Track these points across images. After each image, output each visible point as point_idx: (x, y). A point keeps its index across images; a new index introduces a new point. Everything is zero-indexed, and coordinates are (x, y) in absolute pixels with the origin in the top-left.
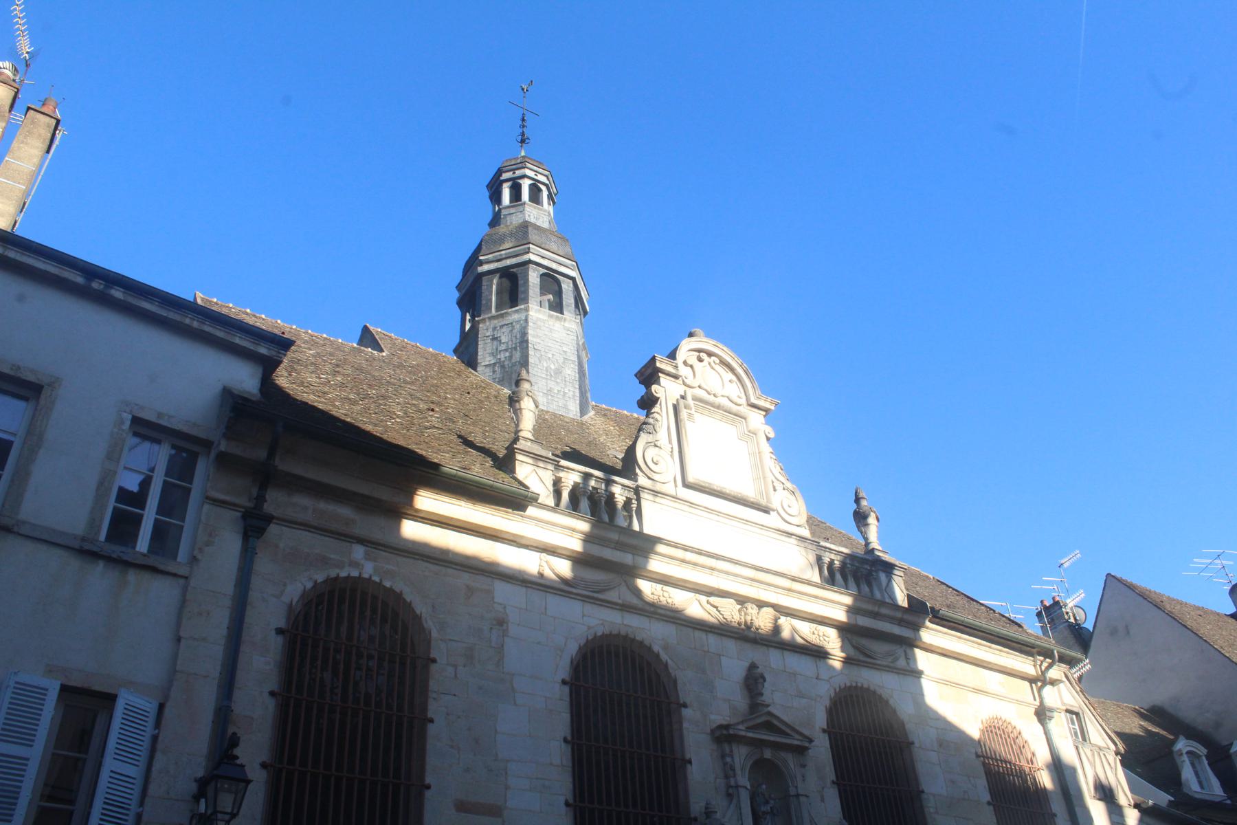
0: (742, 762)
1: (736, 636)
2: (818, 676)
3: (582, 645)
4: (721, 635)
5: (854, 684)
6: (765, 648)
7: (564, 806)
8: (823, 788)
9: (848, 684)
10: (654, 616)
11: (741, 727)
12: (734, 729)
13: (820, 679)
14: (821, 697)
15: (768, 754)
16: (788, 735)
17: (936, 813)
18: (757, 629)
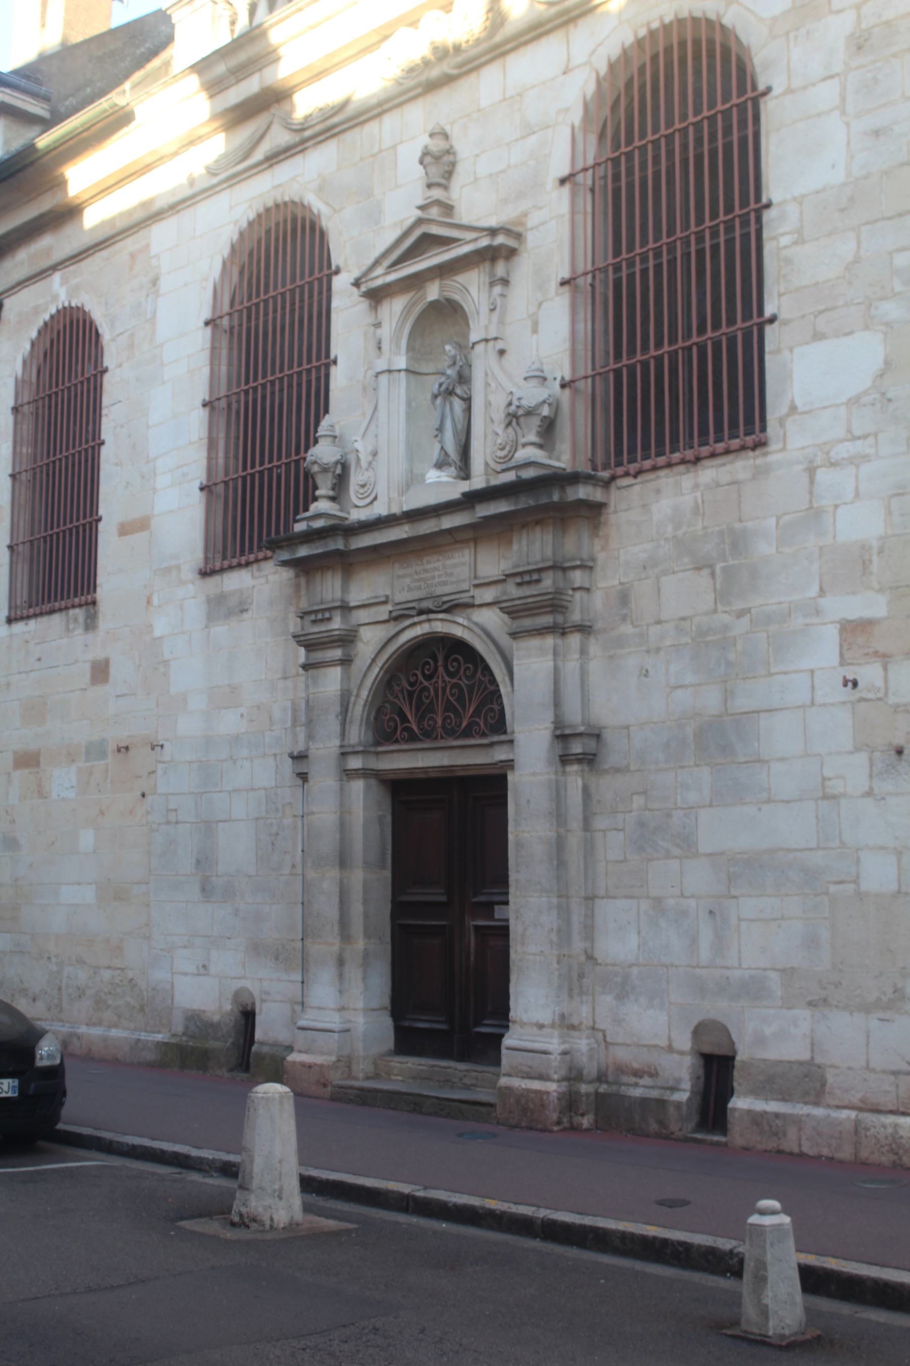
0: (394, 325)
1: (419, 90)
2: (567, 66)
3: (226, 255)
4: (401, 104)
5: (643, 32)
6: (473, 76)
7: (198, 491)
8: (540, 304)
9: (629, 39)
10: (307, 145)
11: (379, 271)
12: (366, 282)
13: (571, 70)
14: (567, 110)
15: (433, 292)
16: (455, 240)
17: (800, 241)
18: (467, 42)
